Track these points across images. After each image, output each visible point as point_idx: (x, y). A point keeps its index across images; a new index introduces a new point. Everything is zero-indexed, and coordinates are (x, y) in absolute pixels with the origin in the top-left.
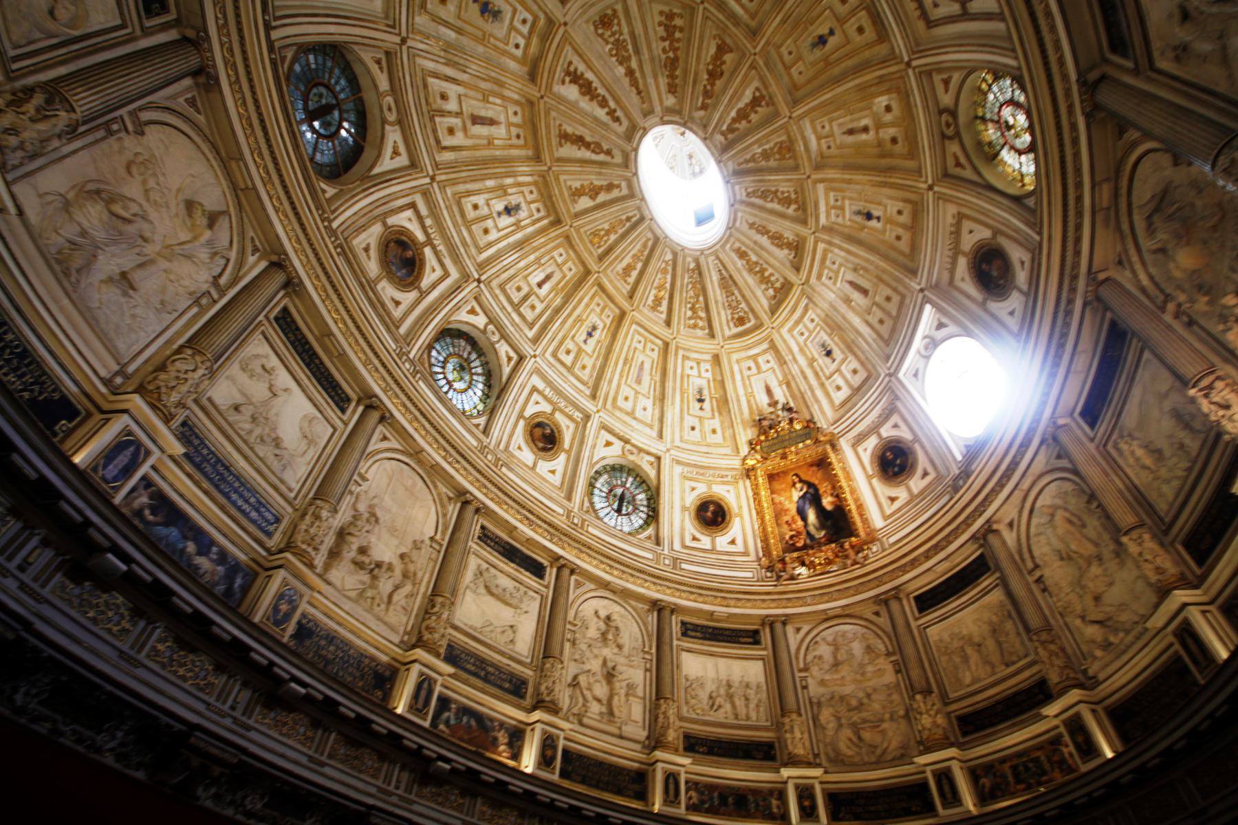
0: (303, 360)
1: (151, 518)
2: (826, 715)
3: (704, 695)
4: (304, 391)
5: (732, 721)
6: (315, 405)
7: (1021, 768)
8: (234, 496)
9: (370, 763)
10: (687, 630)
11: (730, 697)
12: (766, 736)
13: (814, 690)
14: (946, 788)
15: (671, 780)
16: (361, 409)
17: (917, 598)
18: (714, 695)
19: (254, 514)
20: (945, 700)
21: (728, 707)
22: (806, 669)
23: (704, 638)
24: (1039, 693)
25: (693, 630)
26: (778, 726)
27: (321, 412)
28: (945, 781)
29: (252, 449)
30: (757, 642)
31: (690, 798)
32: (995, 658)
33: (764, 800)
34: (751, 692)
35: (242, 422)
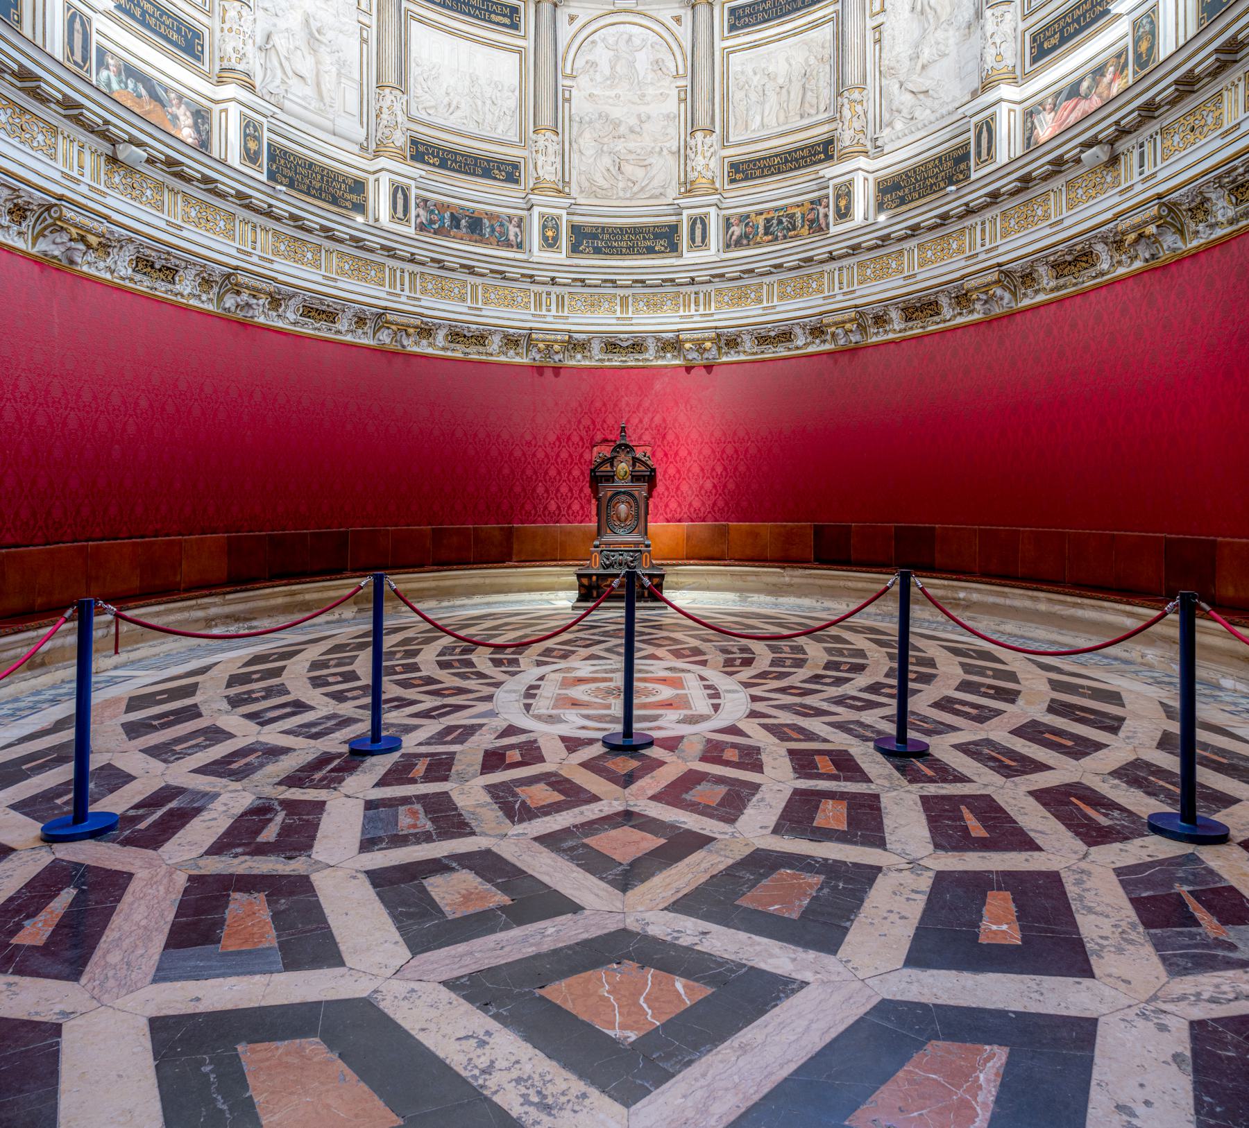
2: (586, 142)
5: (472, 128)
7: (775, 222)
9: (40, 138)
13: (580, 105)
14: (698, 232)
15: (400, 195)
17: (732, 11)
20: (725, 142)
22: (572, 77)
24: (824, 151)
26: (523, 142)
28: (699, 225)
30: (515, 26)
32: (794, 105)
33: (502, 225)
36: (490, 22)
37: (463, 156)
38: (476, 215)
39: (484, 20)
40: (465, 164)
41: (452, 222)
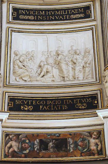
3: (33, 66)
5: (58, 82)
10: (18, 14)
11: (58, 64)
12: (88, 90)
18: (42, 64)
21: (55, 72)
23: (37, 20)
25: (26, 14)
31: (11, 147)
33: (83, 140)
34: (79, 58)
36: (71, 19)
37: (52, 100)
38: (61, 137)
39: (66, 20)
40: (54, 105)
41: (40, 146)
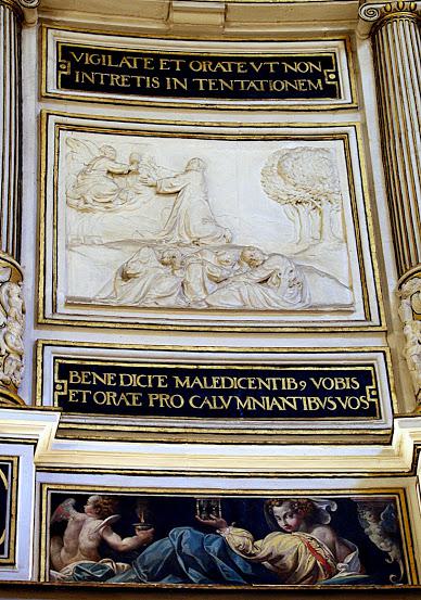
0: (179, 93)
1: (128, 542)
4: (221, 137)
6: (266, 138)
8: (250, 403)
16: (364, 51)
19: (309, 403)
27: (286, 138)
29: (210, 309)
35: (158, 285)
